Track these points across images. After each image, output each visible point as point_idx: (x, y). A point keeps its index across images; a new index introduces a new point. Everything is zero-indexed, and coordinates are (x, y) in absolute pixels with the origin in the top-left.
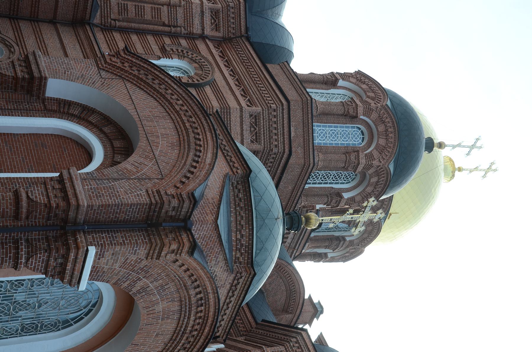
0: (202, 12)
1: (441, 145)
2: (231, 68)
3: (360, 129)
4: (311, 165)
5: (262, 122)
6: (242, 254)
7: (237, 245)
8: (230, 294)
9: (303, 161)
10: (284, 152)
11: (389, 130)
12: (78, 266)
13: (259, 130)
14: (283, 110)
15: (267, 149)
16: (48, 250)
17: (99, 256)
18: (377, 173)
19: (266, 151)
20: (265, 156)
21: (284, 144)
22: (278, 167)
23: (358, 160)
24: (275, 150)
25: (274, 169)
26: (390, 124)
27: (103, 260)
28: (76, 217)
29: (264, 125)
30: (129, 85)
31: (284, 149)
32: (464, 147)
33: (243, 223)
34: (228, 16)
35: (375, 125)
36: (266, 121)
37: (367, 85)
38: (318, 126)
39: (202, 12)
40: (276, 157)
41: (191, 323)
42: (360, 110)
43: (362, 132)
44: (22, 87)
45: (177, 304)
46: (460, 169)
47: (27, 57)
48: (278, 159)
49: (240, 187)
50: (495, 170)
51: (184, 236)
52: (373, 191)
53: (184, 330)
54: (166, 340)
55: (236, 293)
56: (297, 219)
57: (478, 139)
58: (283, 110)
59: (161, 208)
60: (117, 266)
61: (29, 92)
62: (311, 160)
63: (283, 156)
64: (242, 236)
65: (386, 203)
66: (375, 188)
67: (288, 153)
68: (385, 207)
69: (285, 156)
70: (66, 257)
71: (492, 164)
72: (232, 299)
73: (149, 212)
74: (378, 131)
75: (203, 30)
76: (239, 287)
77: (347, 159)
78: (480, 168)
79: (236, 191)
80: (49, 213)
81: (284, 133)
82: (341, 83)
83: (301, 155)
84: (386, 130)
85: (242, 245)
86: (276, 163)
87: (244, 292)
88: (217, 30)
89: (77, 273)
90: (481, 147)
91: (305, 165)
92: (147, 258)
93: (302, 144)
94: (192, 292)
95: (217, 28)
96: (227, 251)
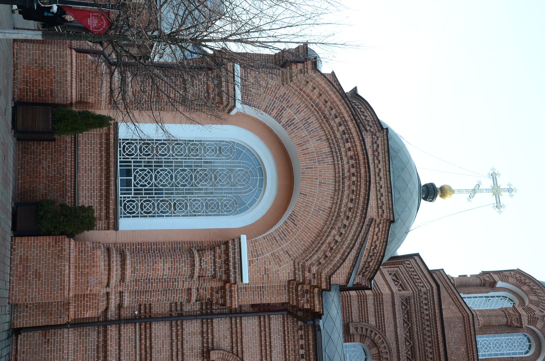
4: (470, 315)
5: (402, 275)
9: (460, 314)
10: (432, 288)
15: (416, 292)
19: (416, 294)
20: (417, 299)
22: (434, 307)
23: (518, 312)
24: (423, 290)
25: (431, 311)
29: (405, 277)
31: (431, 286)
36: (405, 274)
40: (428, 297)
41: (346, 166)
45: (326, 144)
48: (430, 298)
53: (343, 175)
54: (331, 192)
55: (380, 158)
62: (467, 311)
63: (433, 293)
67: (436, 287)
69: (435, 291)
72: (380, 166)
76: (380, 150)
77: (505, 313)
81: (424, 275)
83: (456, 310)
85: (368, 121)
86: (431, 303)
87: (386, 154)
91: (464, 317)
92: (283, 84)
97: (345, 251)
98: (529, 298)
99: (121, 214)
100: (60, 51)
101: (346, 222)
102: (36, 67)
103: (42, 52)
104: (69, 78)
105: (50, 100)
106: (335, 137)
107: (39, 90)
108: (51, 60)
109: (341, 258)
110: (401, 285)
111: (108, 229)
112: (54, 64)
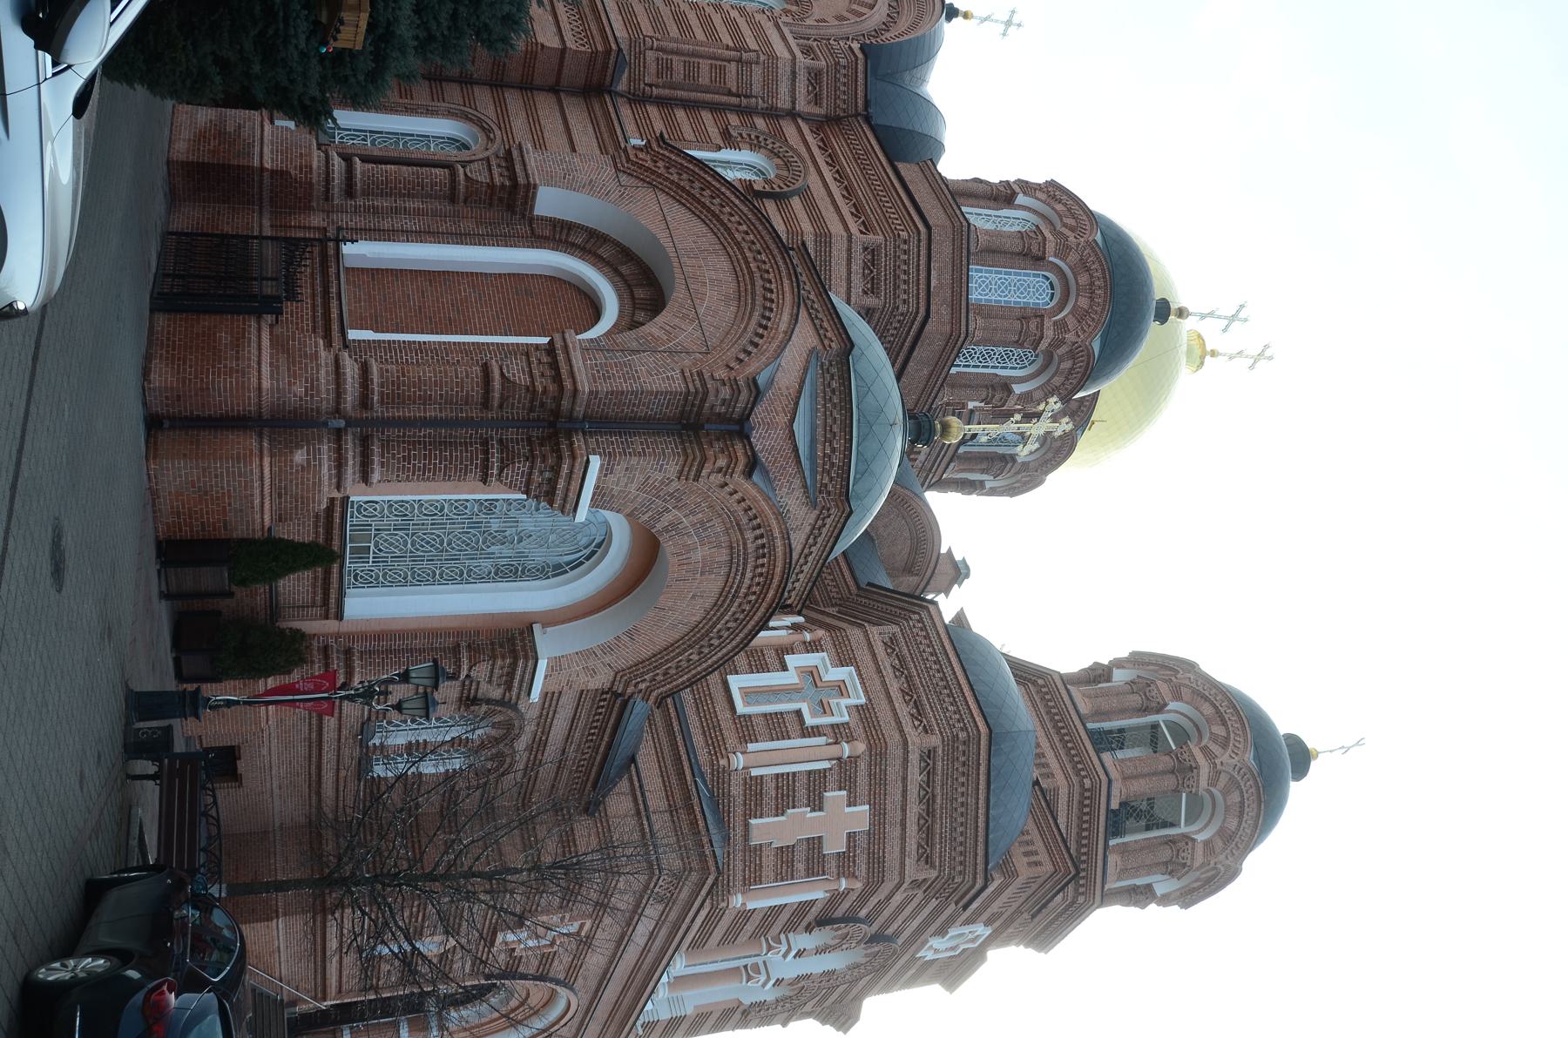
0: (794, 73)
1: (1182, 313)
3: (1047, 279)
6: (831, 479)
7: (824, 464)
8: (811, 541)
9: (948, 328)
10: (917, 312)
12: (575, 485)
13: (878, 274)
14: (919, 241)
16: (531, 457)
17: (606, 471)
18: (1072, 355)
21: (918, 298)
22: (906, 337)
23: (1042, 331)
24: (903, 308)
26: (1099, 274)
28: (572, 409)
29: (886, 265)
30: (662, 197)
31: (918, 308)
32: (1219, 317)
33: (836, 429)
34: (836, 80)
35: (1073, 273)
37: (1065, 205)
38: (977, 271)
39: (794, 73)
41: (747, 582)
42: (1050, 247)
43: (1051, 283)
45: (725, 551)
46: (1213, 354)
47: (509, 152)
49: (834, 370)
50: (1271, 358)
51: (739, 447)
52: (1063, 384)
53: (736, 591)
55: (820, 540)
56: (927, 427)
57: (1242, 306)
58: (919, 241)
59: (703, 400)
60: (633, 488)
61: (511, 208)
63: (915, 319)
64: (833, 450)
66: (1067, 379)
69: (919, 318)
70: (556, 470)
71: (1266, 347)
72: (813, 549)
74: (1077, 283)
75: (794, 103)
76: (824, 530)
79: (828, 376)
81: (918, 280)
82: (1021, 199)
83: (947, 318)
84: (1092, 284)
85: (833, 465)
88: (816, 104)
89: (572, 495)
91: (951, 335)
92: (679, 479)
93: (949, 300)
94: (749, 535)
95: (817, 100)
96: (807, 473)
97: (699, 673)
98: (1077, 300)
99: (349, 584)
100: (239, 468)
101: (716, 642)
102: (194, 492)
103: (204, 470)
104: (257, 502)
105: (223, 535)
106: (745, 548)
107: (203, 523)
108: (222, 479)
109: (689, 680)
111: (327, 618)
112: (228, 485)
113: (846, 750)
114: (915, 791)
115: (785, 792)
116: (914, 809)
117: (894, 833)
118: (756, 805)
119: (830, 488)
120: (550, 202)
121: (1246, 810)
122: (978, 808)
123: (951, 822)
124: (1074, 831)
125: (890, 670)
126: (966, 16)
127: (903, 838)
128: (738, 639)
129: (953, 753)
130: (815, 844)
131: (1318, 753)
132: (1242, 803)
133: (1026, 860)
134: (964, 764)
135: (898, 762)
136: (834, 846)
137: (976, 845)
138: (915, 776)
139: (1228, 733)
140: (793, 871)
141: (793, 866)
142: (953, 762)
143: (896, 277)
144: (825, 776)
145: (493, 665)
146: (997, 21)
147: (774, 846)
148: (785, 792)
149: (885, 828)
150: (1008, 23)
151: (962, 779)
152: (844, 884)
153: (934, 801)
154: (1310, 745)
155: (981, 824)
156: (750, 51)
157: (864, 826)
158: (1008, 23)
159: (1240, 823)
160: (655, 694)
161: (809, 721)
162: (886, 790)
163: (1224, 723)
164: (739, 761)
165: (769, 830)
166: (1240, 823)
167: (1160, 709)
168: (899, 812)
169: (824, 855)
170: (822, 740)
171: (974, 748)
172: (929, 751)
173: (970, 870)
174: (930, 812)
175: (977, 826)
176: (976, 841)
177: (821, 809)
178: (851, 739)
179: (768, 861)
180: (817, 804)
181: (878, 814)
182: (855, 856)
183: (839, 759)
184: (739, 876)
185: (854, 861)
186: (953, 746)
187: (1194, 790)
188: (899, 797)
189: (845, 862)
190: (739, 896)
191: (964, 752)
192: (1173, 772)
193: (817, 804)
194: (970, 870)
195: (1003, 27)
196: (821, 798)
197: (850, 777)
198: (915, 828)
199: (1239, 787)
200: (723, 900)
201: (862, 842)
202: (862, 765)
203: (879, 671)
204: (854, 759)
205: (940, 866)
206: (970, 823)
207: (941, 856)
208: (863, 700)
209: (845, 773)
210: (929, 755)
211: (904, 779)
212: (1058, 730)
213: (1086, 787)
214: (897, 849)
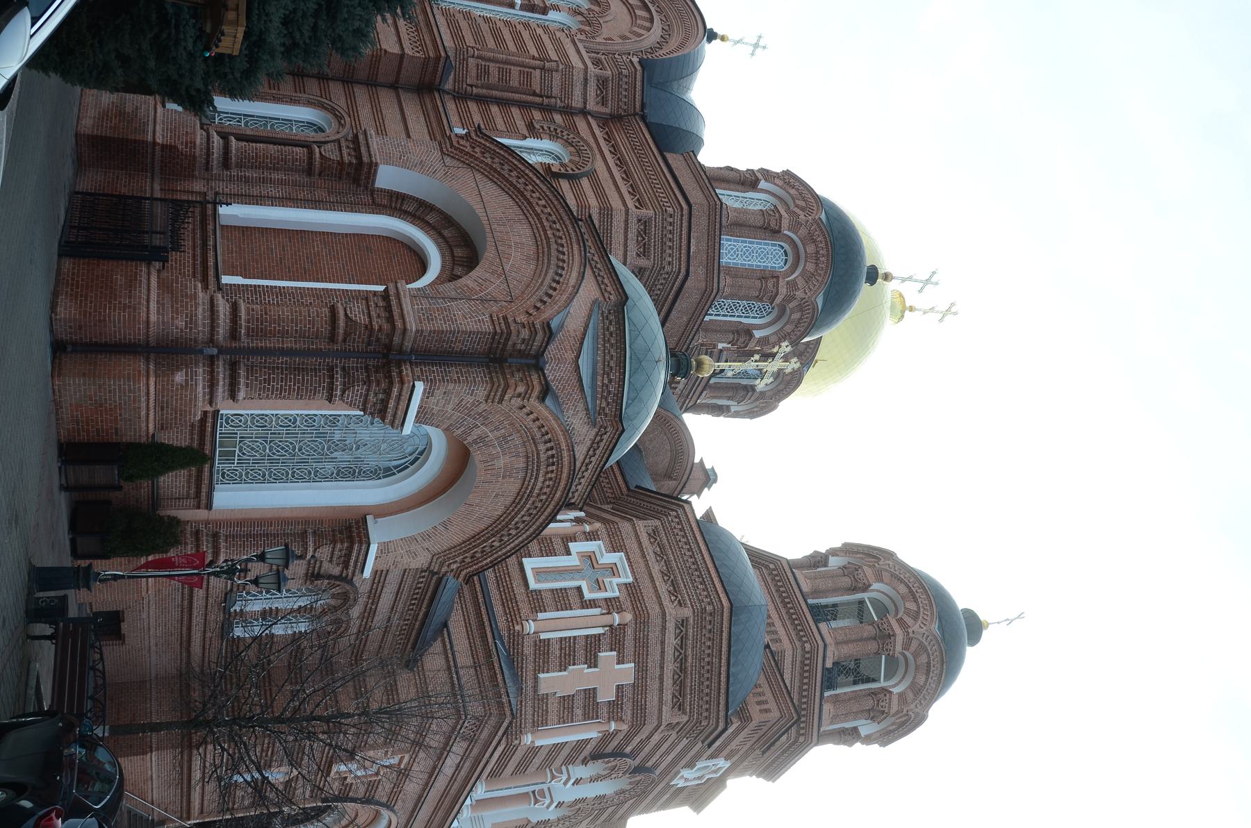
0: (586, 80)
1: (887, 277)
2: (619, 155)
3: (782, 248)
6: (608, 404)
7: (603, 391)
8: (591, 453)
9: (704, 285)
10: (679, 272)
11: (821, 252)
13: (649, 241)
14: (682, 215)
16: (368, 382)
17: (428, 394)
18: (801, 308)
21: (680, 261)
22: (670, 292)
23: (777, 288)
24: (668, 268)
26: (822, 245)
27: (432, 400)
28: (402, 344)
29: (655, 234)
30: (478, 176)
31: (680, 268)
32: (916, 281)
33: (612, 364)
34: (619, 86)
38: (727, 240)
39: (586, 80)
41: (539, 484)
42: (785, 223)
43: (785, 251)
44: (348, 174)
46: (911, 309)
47: (356, 136)
49: (612, 317)
50: (955, 314)
51: (535, 376)
52: (793, 331)
53: (530, 492)
54: (507, 503)
55: (598, 452)
56: (685, 363)
57: (934, 273)
58: (682, 215)
59: (507, 339)
61: (356, 181)
63: (677, 277)
64: (610, 381)
65: (812, 346)
66: (796, 327)
68: (810, 351)
70: (388, 393)
71: (953, 304)
72: (593, 459)
73: (492, 343)
74: (806, 252)
75: (585, 103)
76: (602, 444)
78: (936, 309)
80: (370, 336)
81: (681, 246)
82: (763, 184)
84: (817, 252)
85: (609, 392)
87: (608, 452)
88: (603, 105)
89: (400, 413)
90: (937, 284)
91: (706, 290)
92: (486, 401)
94: (542, 447)
95: (604, 102)
96: (589, 399)
97: (500, 556)
100: (129, 386)
101: (513, 532)
102: (91, 404)
103: (100, 387)
104: (143, 413)
105: (115, 439)
106: (538, 458)
107: (98, 430)
108: (115, 395)
109: (491, 562)
110: (645, 244)
111: (199, 508)
112: (120, 399)
113: (617, 619)
114: (671, 652)
115: (568, 653)
116: (670, 667)
117: (653, 685)
118: (544, 662)
119: (607, 411)
120: (388, 177)
121: (932, 668)
122: (721, 666)
123: (700, 677)
124: (797, 684)
125: (652, 556)
126: (723, 38)
127: (661, 690)
128: (531, 530)
129: (701, 622)
130: (590, 694)
131: (988, 624)
132: (929, 663)
133: (758, 708)
134: (710, 631)
135: (658, 629)
136: (606, 695)
137: (719, 696)
138: (671, 640)
139: (919, 608)
140: (572, 715)
141: (573, 711)
142: (701, 630)
143: (663, 243)
144: (599, 640)
145: (334, 548)
146: (747, 44)
147: (558, 695)
148: (568, 653)
149: (646, 682)
150: (756, 46)
151: (709, 643)
152: (613, 726)
153: (686, 660)
154: (982, 618)
155: (723, 679)
156: (552, 61)
157: (630, 680)
158: (756, 46)
159: (927, 679)
160: (464, 573)
161: (588, 595)
162: (648, 651)
163: (916, 600)
164: (531, 627)
165: (555, 682)
166: (927, 679)
167: (866, 588)
168: (658, 669)
169: (598, 703)
170: (597, 611)
171: (717, 618)
172: (683, 621)
173: (713, 715)
174: (682, 669)
175: (720, 681)
176: (719, 692)
177: (596, 666)
178: (620, 610)
179: (553, 707)
180: (592, 662)
181: (641, 670)
182: (622, 704)
183: (611, 626)
184: (529, 717)
185: (622, 709)
186: (702, 617)
187: (891, 653)
188: (658, 657)
189: (615, 709)
190: (529, 735)
191: (710, 621)
192: (875, 639)
193: (592, 662)
194: (713, 715)
195: (752, 48)
196: (596, 657)
197: (620, 641)
198: (670, 681)
199: (926, 651)
200: (516, 739)
201: (628, 693)
202: (629, 631)
203: (644, 556)
204: (622, 626)
205: (690, 712)
206: (715, 679)
207: (690, 705)
208: (631, 580)
209: (615, 637)
210: (683, 623)
211: (663, 642)
212: (785, 604)
213: (807, 650)
214: (656, 699)
